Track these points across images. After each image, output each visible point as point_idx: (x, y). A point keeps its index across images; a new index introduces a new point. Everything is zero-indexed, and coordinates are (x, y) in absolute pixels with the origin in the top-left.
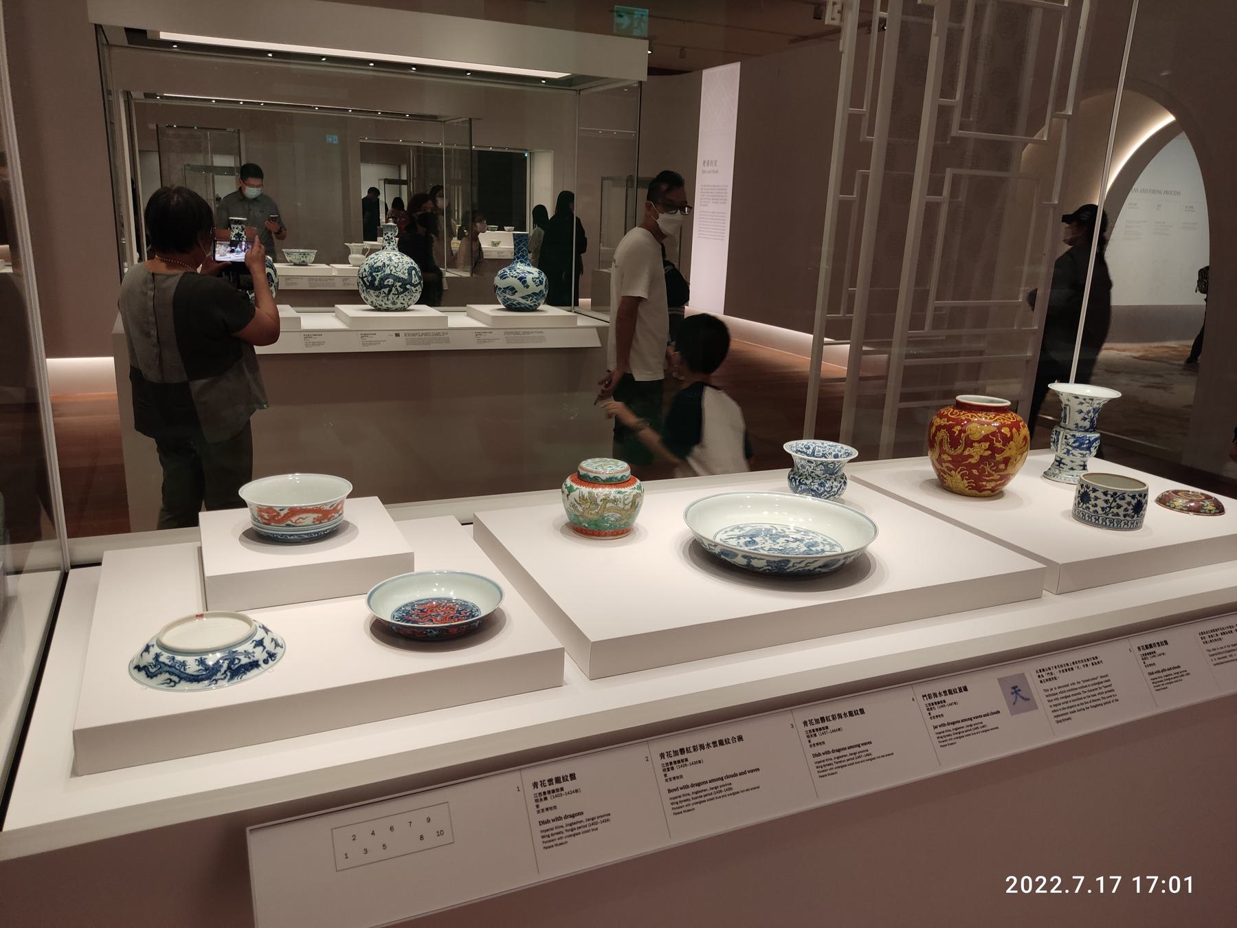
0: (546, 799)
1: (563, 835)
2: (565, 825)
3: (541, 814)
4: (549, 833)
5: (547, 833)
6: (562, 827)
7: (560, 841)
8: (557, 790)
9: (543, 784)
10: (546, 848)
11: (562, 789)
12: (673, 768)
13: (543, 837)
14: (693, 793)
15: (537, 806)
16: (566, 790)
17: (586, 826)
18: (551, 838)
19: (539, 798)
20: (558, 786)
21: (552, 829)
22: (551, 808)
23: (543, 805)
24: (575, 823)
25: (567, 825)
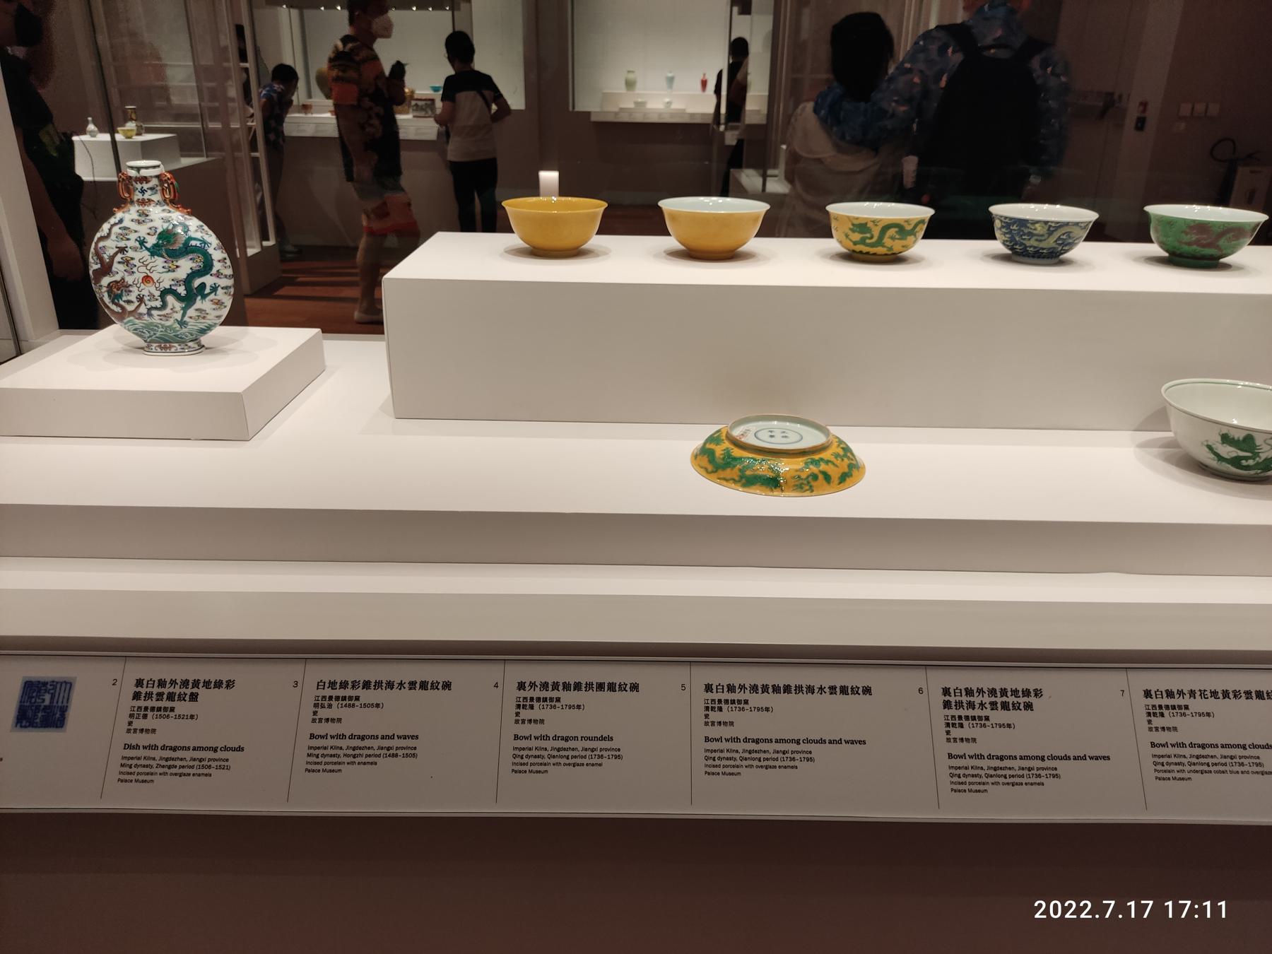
0: (330, 706)
6: (341, 748)
8: (351, 698)
9: (332, 685)
11: (357, 698)
12: (532, 707)
14: (348, 748)
16: (362, 701)
21: (325, 748)
22: (333, 720)
23: (323, 713)
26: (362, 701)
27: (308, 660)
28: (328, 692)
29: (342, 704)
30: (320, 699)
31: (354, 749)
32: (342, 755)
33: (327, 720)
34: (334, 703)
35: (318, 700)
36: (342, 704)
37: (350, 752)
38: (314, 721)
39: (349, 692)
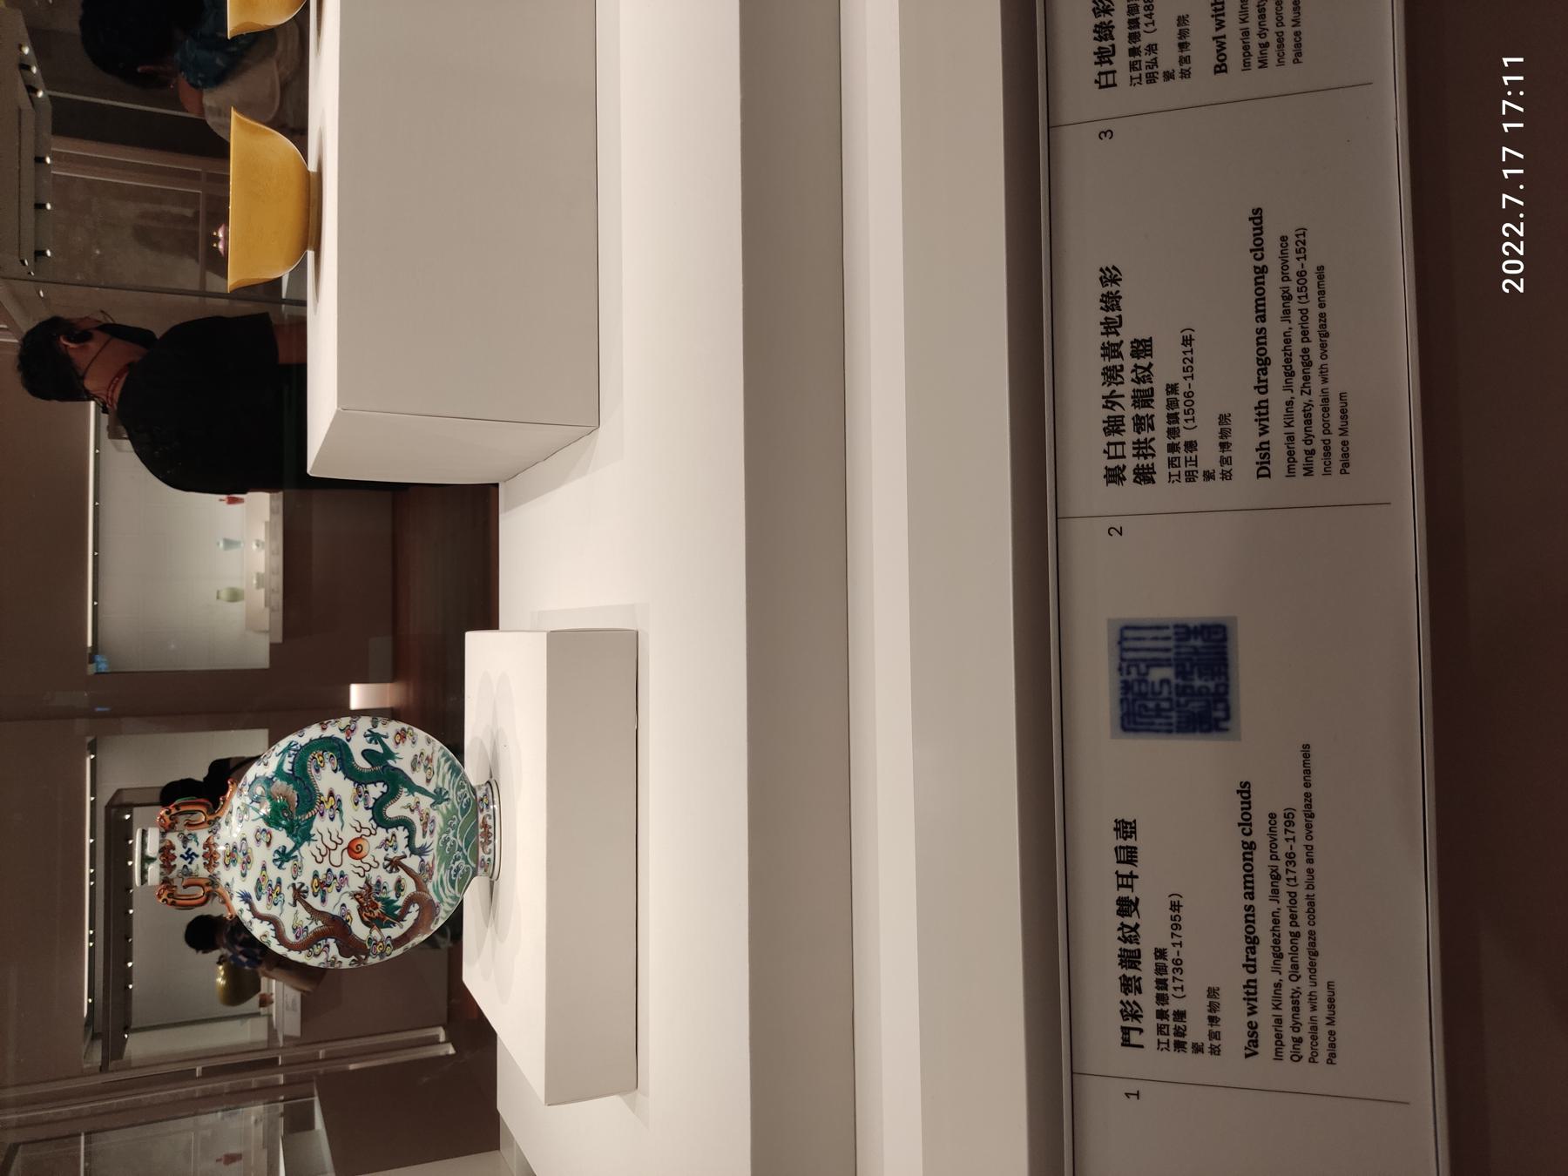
0: (1180, 1015)
2: (1276, 978)
3: (1224, 1043)
6: (1278, 985)
7: (1322, 1003)
8: (1160, 969)
9: (1131, 1013)
10: (1333, 1055)
11: (1160, 953)
15: (1198, 1049)
16: (1165, 942)
18: (1305, 1032)
19: (1172, 1038)
20: (1148, 962)
21: (1279, 1021)
22: (1213, 1007)
23: (1197, 1030)
25: (1276, 969)
29: (1175, 988)
30: (1163, 1039)
31: (1278, 956)
32: (1294, 985)
33: (1213, 1020)
34: (1173, 1005)
35: (1168, 1043)
36: (1175, 988)
37: (1286, 964)
38: (1215, 1051)
39: (1147, 972)
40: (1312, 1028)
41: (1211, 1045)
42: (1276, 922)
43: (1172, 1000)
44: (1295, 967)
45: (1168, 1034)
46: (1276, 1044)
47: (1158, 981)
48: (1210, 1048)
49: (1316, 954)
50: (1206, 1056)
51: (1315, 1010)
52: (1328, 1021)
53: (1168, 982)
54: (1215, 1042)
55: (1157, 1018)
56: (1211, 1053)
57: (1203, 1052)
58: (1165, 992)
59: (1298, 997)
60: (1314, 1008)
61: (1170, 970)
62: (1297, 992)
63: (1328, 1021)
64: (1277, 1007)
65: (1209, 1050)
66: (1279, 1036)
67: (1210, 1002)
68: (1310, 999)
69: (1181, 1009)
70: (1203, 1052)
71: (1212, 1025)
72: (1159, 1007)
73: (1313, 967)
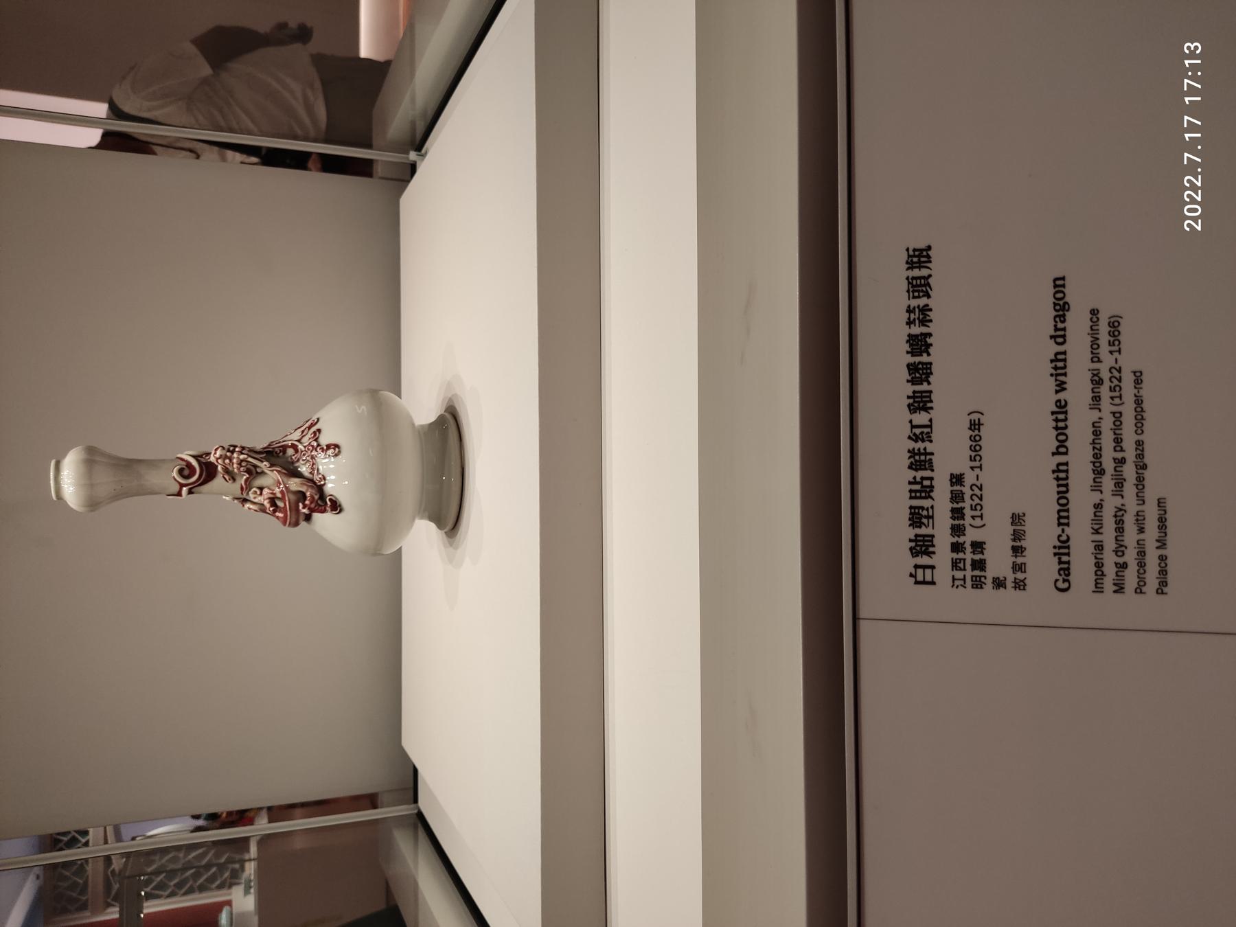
0: (978, 546)
1: (1132, 505)
2: (1096, 497)
3: (1030, 576)
4: (1109, 559)
5: (1110, 570)
6: (1098, 506)
8: (956, 497)
9: (922, 546)
11: (957, 479)
13: (1119, 588)
15: (999, 583)
16: (961, 464)
17: (1118, 416)
18: (1131, 557)
20: (942, 490)
21: (1099, 547)
22: (1017, 536)
23: (998, 562)
24: (1097, 456)
25: (1097, 487)
26: (961, 464)
27: (857, 617)
28: (942, 555)
29: (973, 517)
30: (959, 574)
31: (1099, 472)
32: (1118, 501)
33: (1017, 550)
34: (971, 535)
35: (964, 580)
36: (973, 517)
37: (1108, 483)
38: (1020, 585)
40: (1140, 553)
41: (1015, 579)
42: (1097, 433)
43: (969, 530)
44: (1119, 484)
45: (965, 570)
46: (1096, 575)
47: (953, 510)
48: (1015, 582)
49: (1144, 467)
50: (1009, 592)
51: (1143, 532)
52: (1159, 544)
53: (965, 511)
54: (1020, 576)
55: (953, 551)
56: (1015, 588)
57: (1005, 588)
58: (961, 522)
59: (1123, 515)
60: (1141, 530)
61: (967, 497)
62: (1121, 510)
63: (1159, 544)
64: (1097, 532)
65: (1013, 585)
66: (1099, 565)
67: (1014, 530)
68: (1137, 520)
69: (979, 539)
70: (1005, 588)
71: (1016, 556)
72: (955, 539)
73: (1140, 480)
